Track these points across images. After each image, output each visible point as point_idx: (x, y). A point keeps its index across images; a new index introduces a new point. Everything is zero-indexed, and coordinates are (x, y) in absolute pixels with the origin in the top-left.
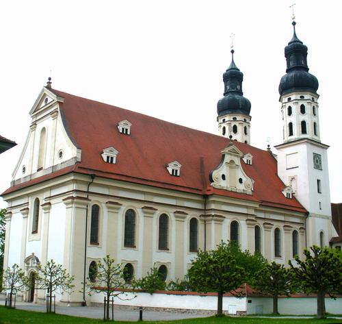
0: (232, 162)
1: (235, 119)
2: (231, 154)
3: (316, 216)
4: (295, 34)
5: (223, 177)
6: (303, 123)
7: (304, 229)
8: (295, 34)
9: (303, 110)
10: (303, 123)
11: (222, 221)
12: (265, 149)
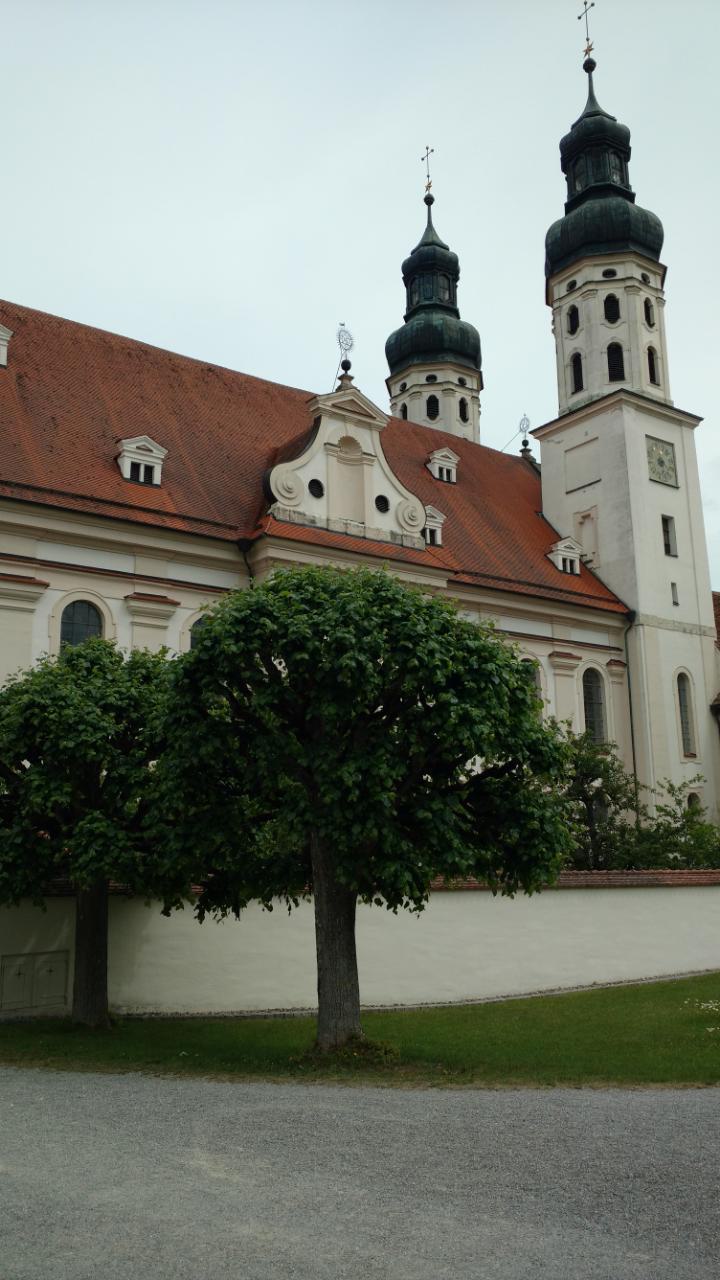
0: (348, 442)
1: (431, 379)
2: (343, 419)
3: (661, 624)
4: (592, 98)
5: (316, 488)
6: (615, 352)
7: (623, 663)
8: (592, 98)
9: (612, 309)
10: (615, 352)
12: (515, 450)
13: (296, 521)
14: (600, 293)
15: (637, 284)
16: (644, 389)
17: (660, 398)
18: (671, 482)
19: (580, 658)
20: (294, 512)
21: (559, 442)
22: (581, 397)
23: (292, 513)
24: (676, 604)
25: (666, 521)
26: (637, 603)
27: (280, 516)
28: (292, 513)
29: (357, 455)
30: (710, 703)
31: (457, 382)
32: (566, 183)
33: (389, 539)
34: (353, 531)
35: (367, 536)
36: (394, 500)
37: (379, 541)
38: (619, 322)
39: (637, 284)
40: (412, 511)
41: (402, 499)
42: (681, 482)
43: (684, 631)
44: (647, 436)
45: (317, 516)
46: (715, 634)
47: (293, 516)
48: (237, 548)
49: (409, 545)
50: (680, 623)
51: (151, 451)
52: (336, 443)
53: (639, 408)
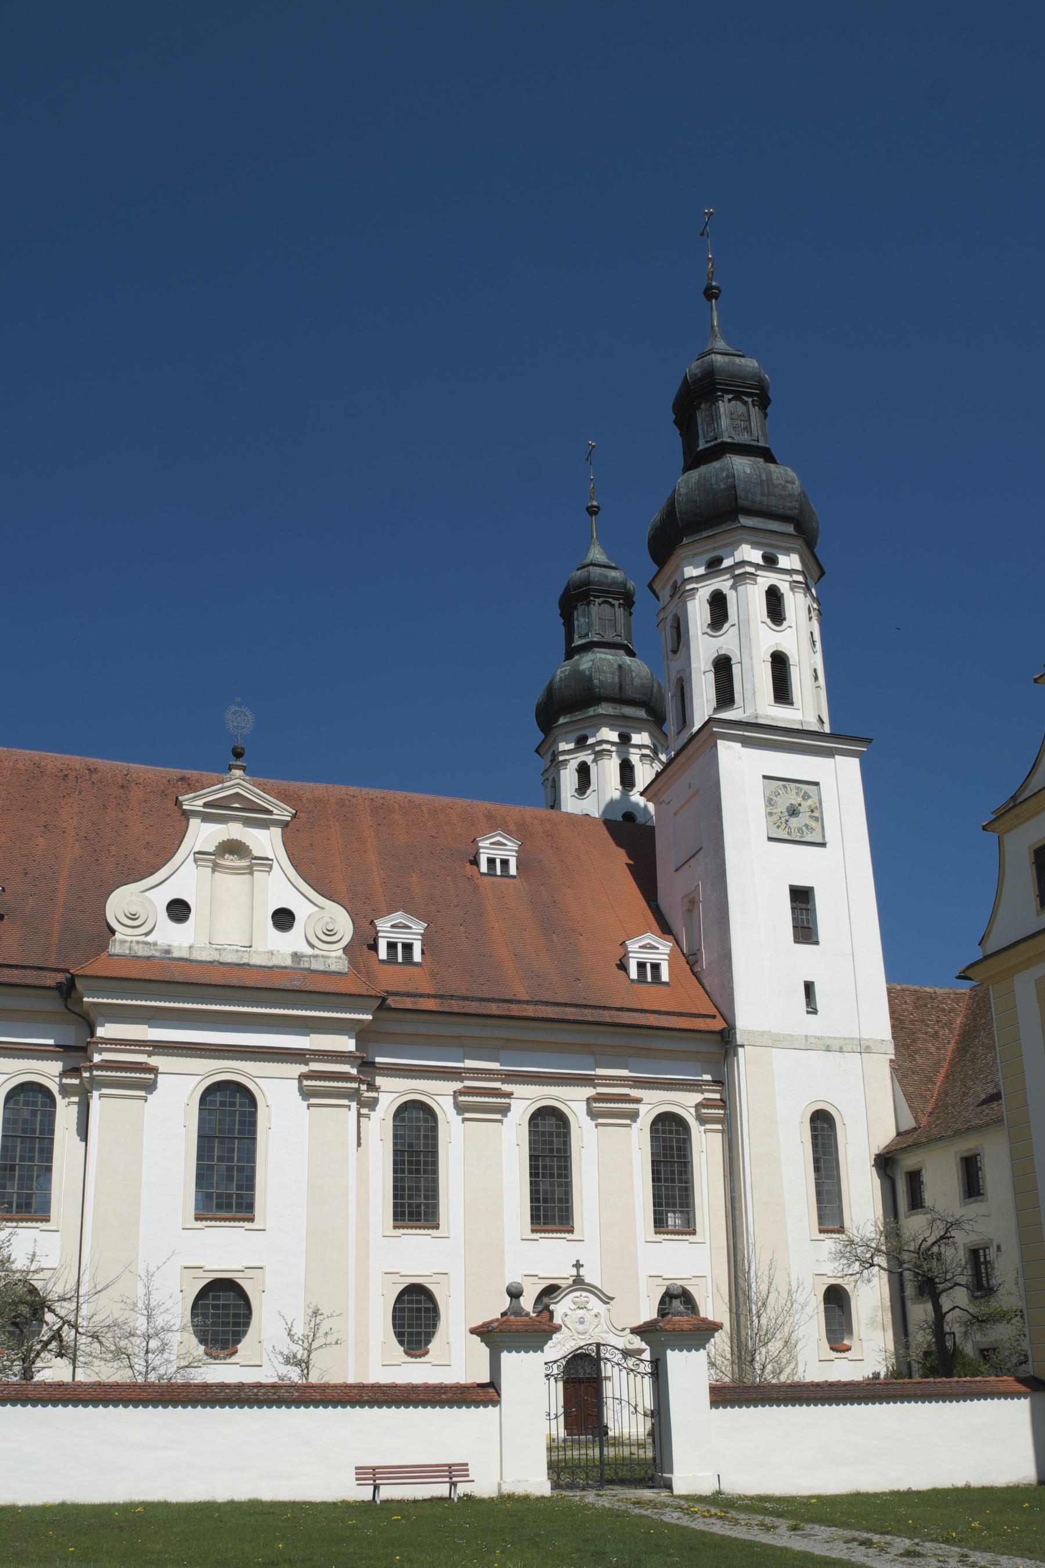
11: (150, 1087)
13: (140, 954)
16: (760, 712)
19: (638, 1101)
20: (138, 942)
23: (134, 944)
28: (134, 944)
33: (288, 962)
35: (252, 962)
36: (302, 910)
40: (327, 923)
41: (317, 909)
42: (831, 834)
43: (828, 1049)
45: (175, 944)
46: (891, 1049)
47: (135, 947)
48: (56, 993)
49: (322, 968)
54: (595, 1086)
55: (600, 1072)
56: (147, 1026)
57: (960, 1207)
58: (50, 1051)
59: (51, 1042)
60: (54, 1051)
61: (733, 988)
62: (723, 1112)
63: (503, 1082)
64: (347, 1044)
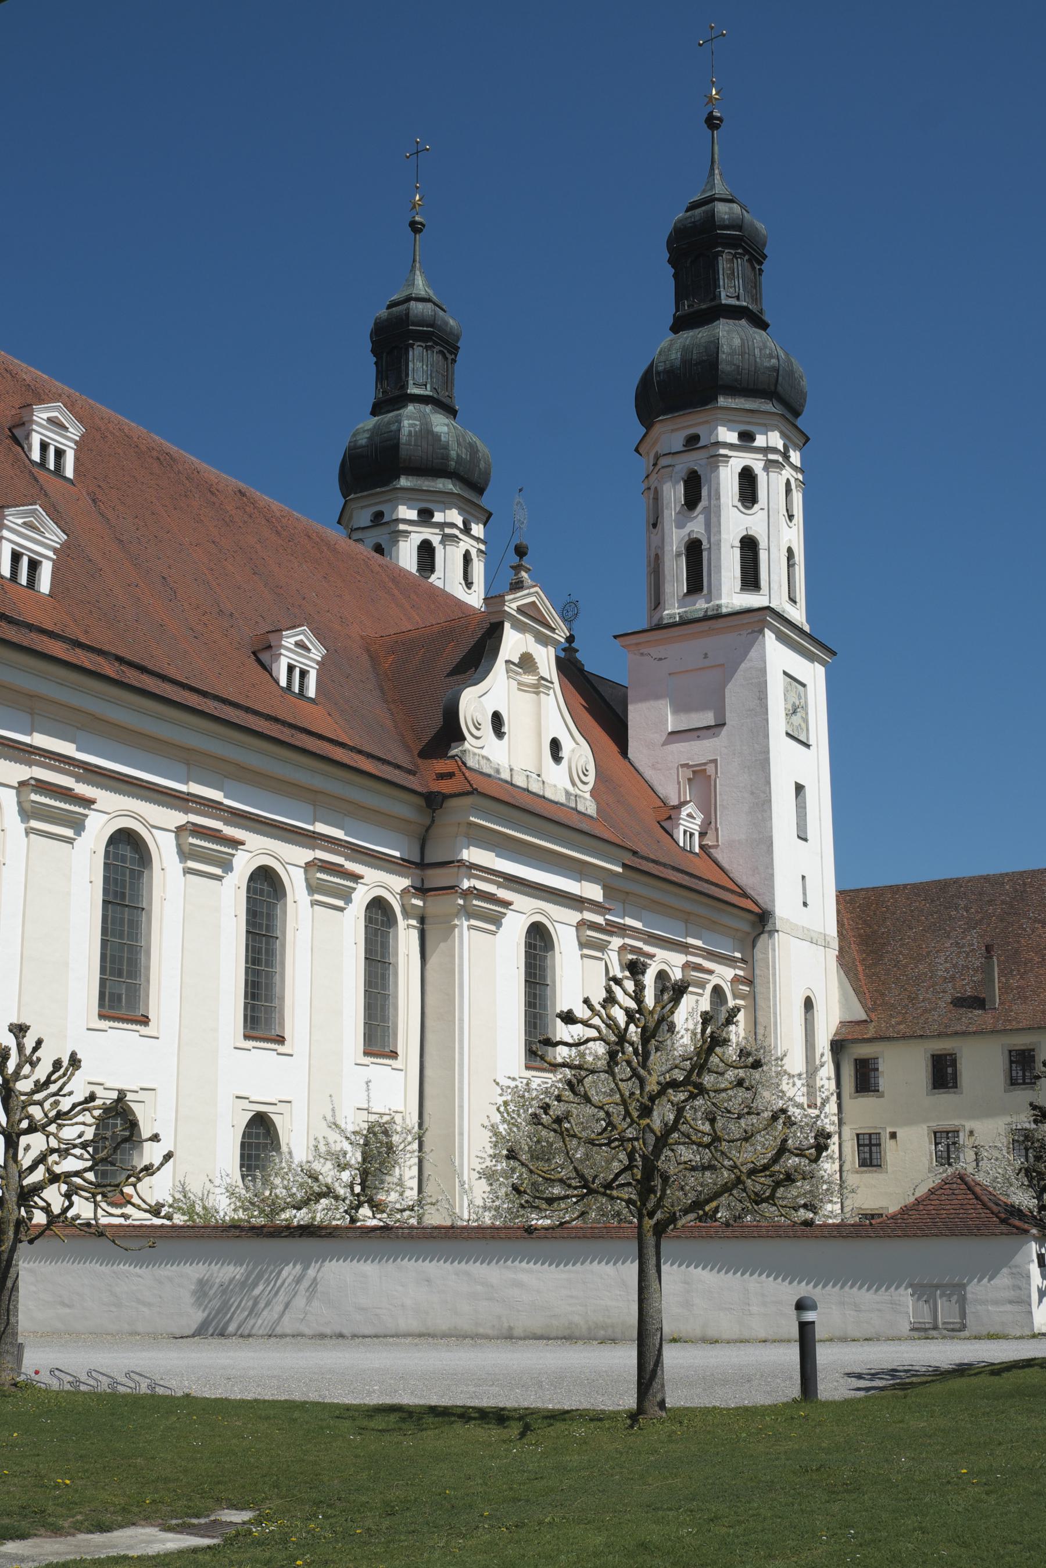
0: (527, 662)
6: (749, 546)
10: (749, 546)
11: (496, 920)
13: (484, 771)
14: (732, 461)
15: (781, 460)
17: (797, 621)
18: (803, 738)
20: (483, 757)
21: (660, 659)
22: (700, 605)
24: (805, 904)
25: (799, 788)
26: (773, 901)
27: (471, 762)
29: (530, 679)
30: (830, 1038)
31: (461, 526)
32: (672, 282)
33: (562, 799)
34: (535, 787)
37: (557, 803)
38: (756, 507)
39: (781, 460)
44: (785, 673)
46: (835, 944)
47: (483, 762)
48: (422, 803)
50: (808, 930)
51: (308, 650)
52: (516, 661)
53: (782, 638)
54: (687, 953)
55: (691, 941)
56: (494, 854)
57: (927, 1095)
58: (397, 863)
59: (397, 854)
60: (400, 864)
61: (772, 875)
62: (748, 989)
63: (646, 942)
64: (594, 892)
